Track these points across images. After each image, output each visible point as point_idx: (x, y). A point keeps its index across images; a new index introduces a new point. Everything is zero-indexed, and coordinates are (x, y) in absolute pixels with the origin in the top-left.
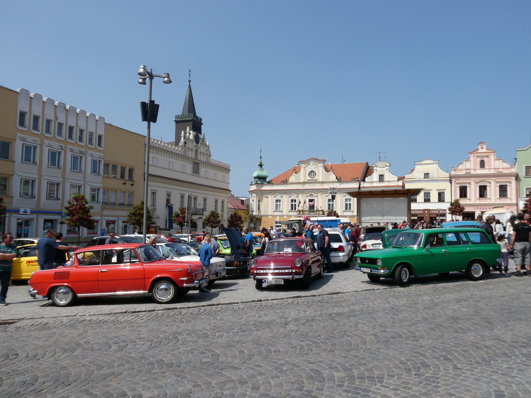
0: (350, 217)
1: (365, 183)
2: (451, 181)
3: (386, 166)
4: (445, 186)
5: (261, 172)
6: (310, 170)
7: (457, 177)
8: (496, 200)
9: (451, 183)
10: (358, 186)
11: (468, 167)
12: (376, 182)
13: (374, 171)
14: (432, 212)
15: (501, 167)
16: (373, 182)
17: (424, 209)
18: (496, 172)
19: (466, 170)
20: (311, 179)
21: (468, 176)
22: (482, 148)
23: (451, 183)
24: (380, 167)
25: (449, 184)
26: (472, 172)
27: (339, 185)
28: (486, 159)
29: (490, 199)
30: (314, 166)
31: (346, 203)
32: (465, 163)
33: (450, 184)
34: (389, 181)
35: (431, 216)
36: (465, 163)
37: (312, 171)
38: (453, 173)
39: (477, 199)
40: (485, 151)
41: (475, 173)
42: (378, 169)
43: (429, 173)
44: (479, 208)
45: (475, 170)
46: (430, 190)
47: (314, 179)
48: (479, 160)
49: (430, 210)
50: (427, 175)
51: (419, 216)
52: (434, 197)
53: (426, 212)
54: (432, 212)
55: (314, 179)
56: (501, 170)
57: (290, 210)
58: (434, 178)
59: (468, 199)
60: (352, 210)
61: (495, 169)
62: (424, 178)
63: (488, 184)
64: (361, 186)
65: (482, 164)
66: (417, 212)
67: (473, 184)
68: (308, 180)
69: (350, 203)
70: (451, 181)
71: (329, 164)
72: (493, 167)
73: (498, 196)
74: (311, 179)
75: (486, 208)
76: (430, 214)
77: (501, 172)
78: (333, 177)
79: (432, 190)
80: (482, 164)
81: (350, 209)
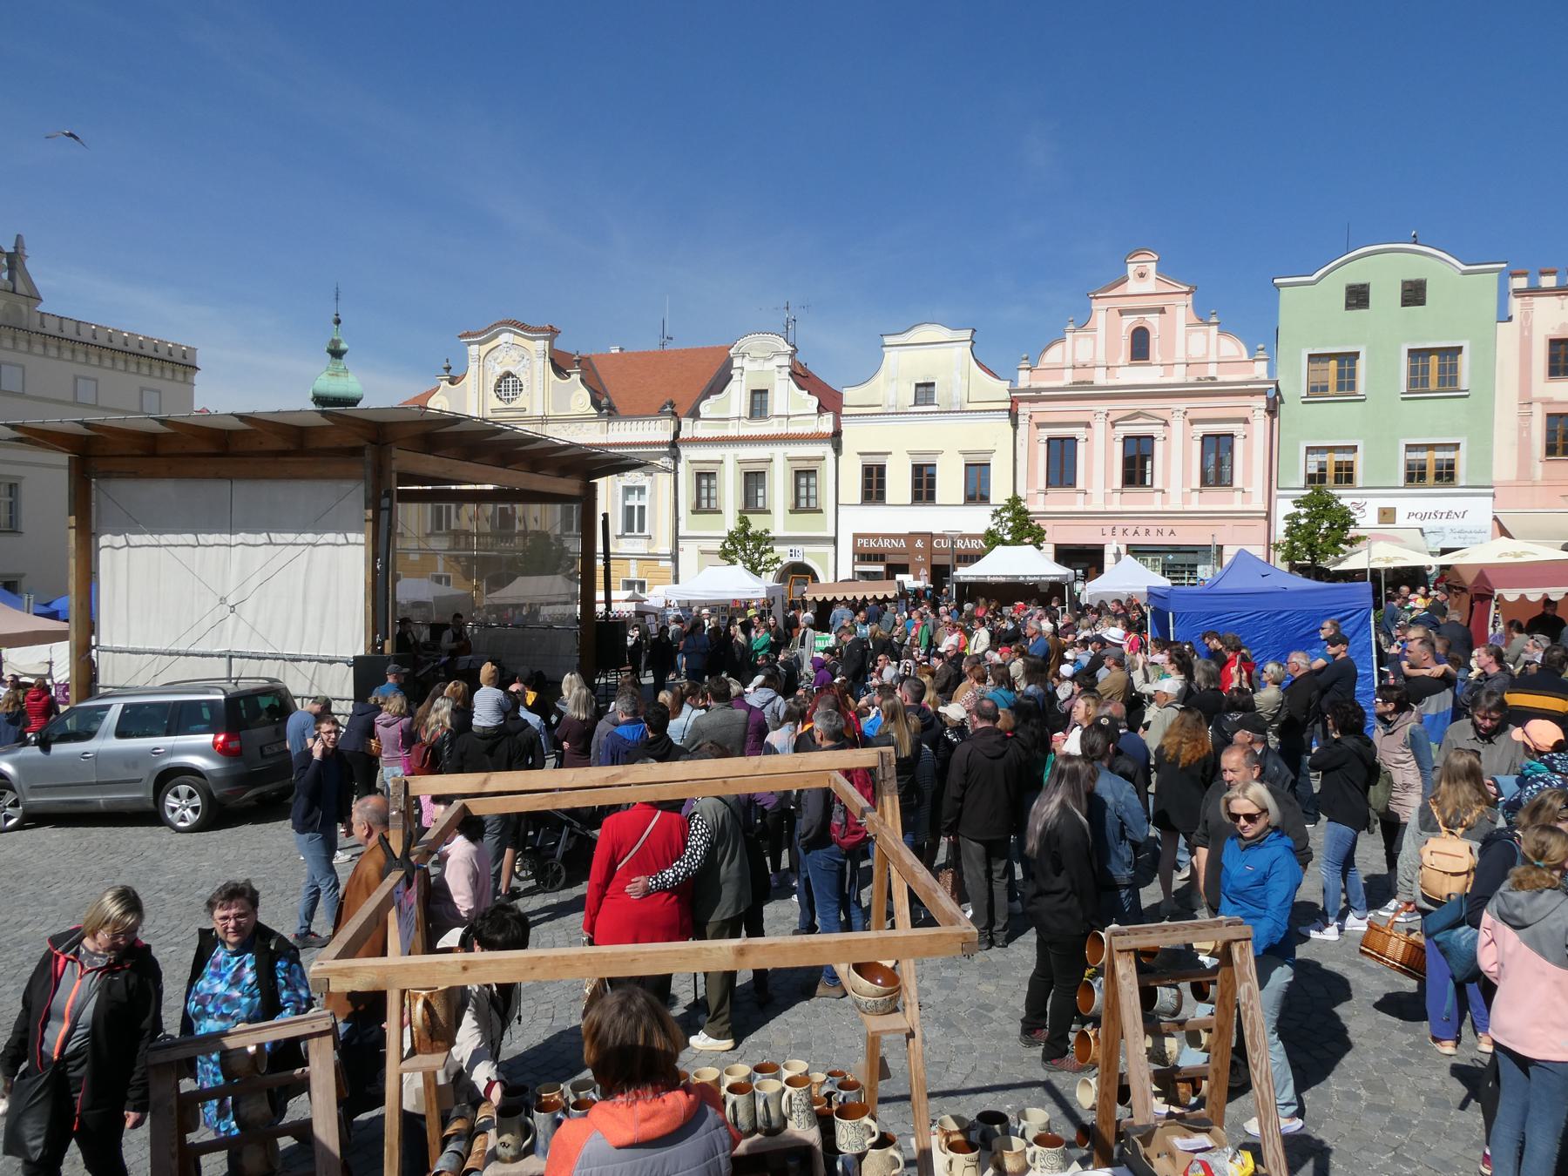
0: (638, 559)
1: (699, 423)
2: (1013, 416)
3: (778, 354)
4: (992, 436)
5: (334, 380)
6: (500, 371)
7: (1037, 396)
8: (1185, 500)
9: (1015, 425)
10: (668, 437)
11: (1083, 357)
12: (739, 418)
13: (731, 377)
14: (938, 544)
15: (1213, 358)
16: (727, 419)
17: (911, 534)
18: (1191, 379)
19: (1074, 367)
20: (502, 405)
21: (1084, 392)
22: (1142, 275)
23: (1015, 425)
24: (754, 359)
25: (1007, 424)
26: (1100, 378)
27: (602, 432)
28: (1153, 322)
29: (1163, 492)
30: (514, 353)
31: (628, 503)
32: (1074, 340)
33: (1011, 430)
34: (788, 417)
35: (938, 560)
36: (1074, 340)
37: (508, 374)
38: (1024, 380)
39: (1115, 491)
40: (1153, 290)
41: (1112, 382)
42: (746, 363)
43: (932, 384)
44: (1119, 531)
45: (1108, 368)
46: (937, 453)
47: (512, 405)
48: (1130, 322)
49: (931, 535)
50: (925, 390)
51: (892, 560)
52: (950, 483)
53: (919, 544)
54: (938, 544)
55: (512, 405)
56: (1212, 371)
57: (428, 531)
58: (951, 404)
59: (1079, 492)
60: (646, 533)
61: (1188, 365)
62: (916, 404)
63: (1156, 430)
64: (682, 436)
65: (1140, 346)
66: (886, 544)
67: (1100, 427)
68: (493, 411)
69: (641, 503)
70: (1013, 416)
71: (613, 351)
72: (1180, 355)
73: (1196, 481)
74: (502, 405)
75: (1147, 532)
76: (931, 552)
77: (1213, 378)
78: (581, 400)
79: (890, 453)
80: (1140, 346)
81: (641, 529)
